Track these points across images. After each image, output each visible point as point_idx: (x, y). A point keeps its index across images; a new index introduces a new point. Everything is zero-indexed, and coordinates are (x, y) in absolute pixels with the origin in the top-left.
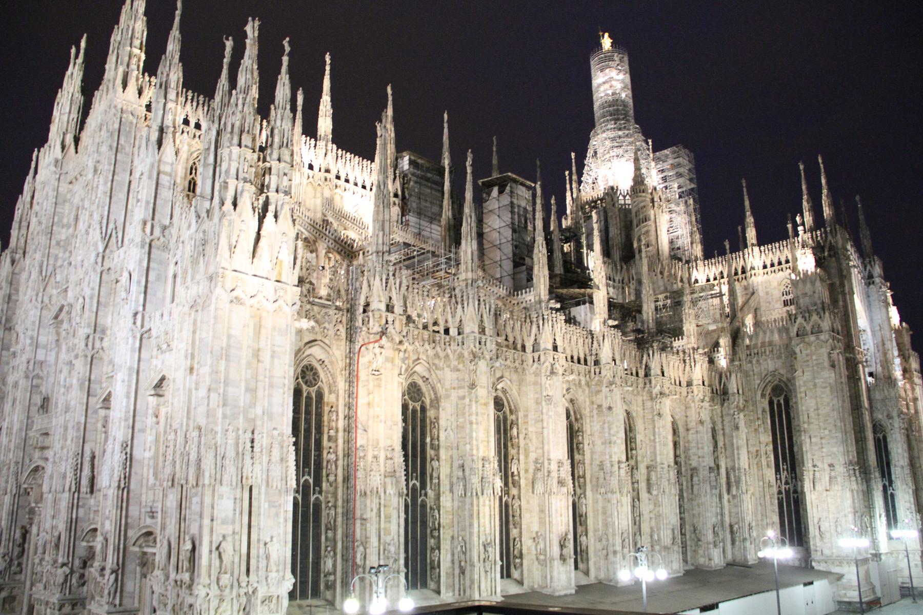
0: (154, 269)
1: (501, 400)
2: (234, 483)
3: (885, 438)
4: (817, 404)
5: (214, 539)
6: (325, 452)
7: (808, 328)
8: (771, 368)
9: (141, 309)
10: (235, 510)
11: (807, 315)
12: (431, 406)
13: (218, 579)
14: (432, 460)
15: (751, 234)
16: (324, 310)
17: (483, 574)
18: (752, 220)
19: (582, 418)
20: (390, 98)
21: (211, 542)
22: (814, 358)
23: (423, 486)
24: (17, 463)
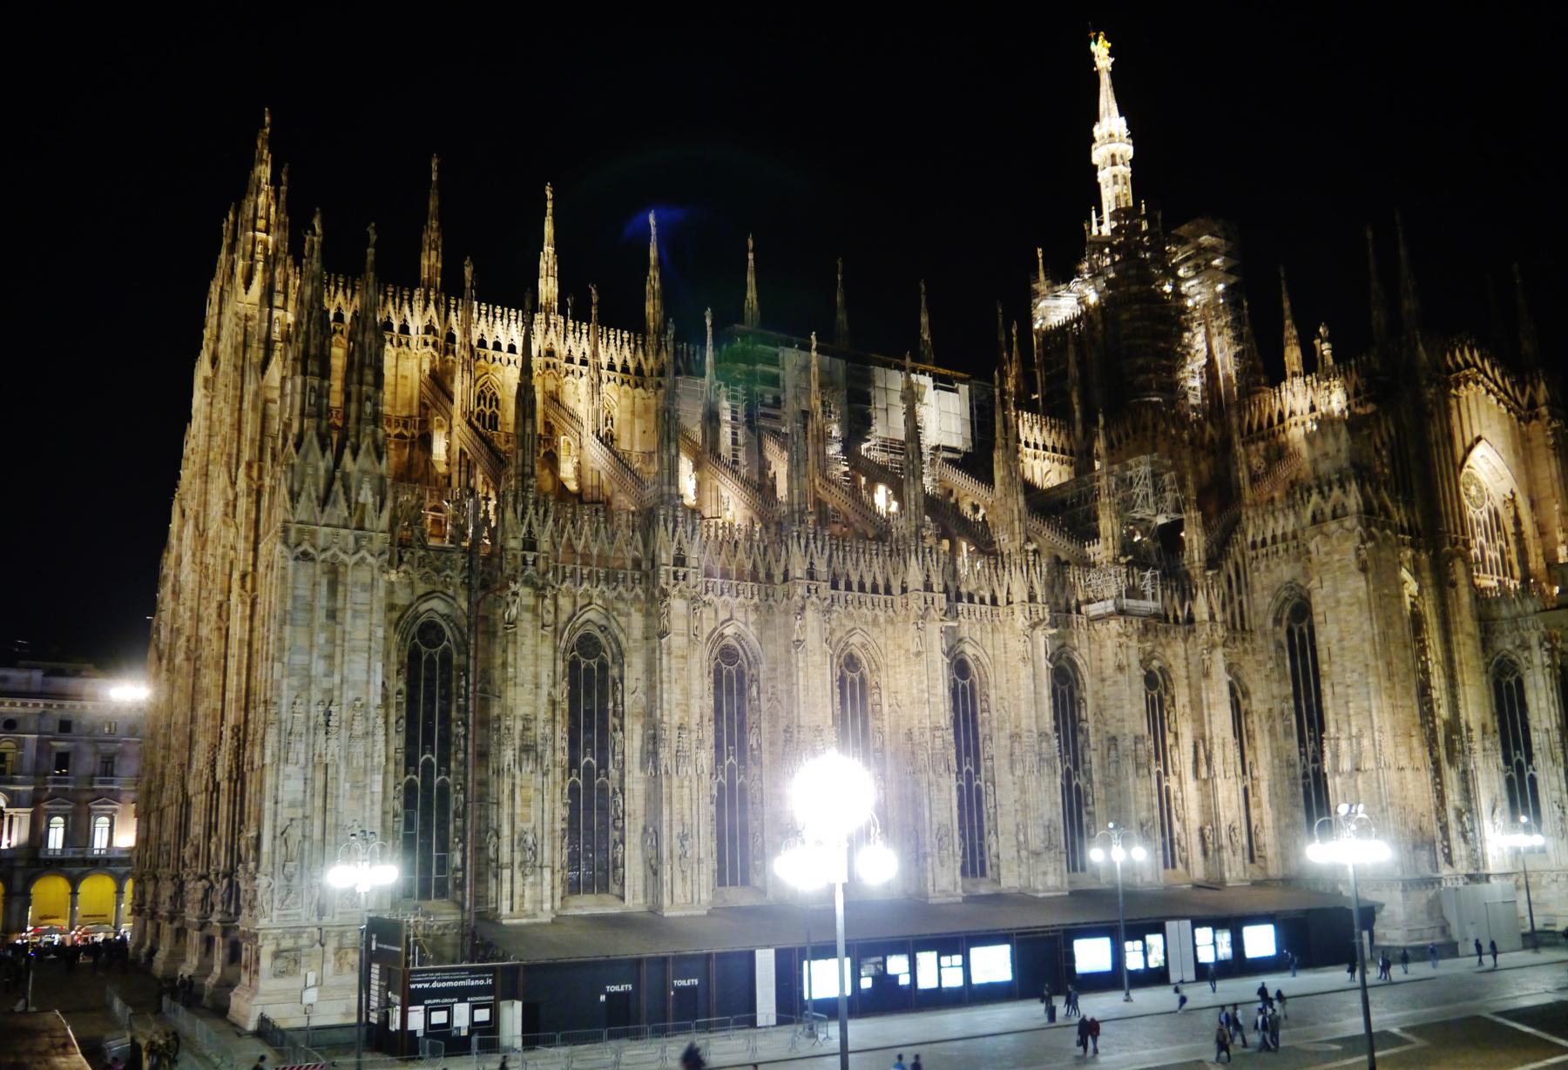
3: (1520, 683)
4: (1341, 631)
7: (1328, 510)
8: (1287, 577)
11: (1326, 489)
16: (444, 556)
17: (678, 876)
21: (275, 827)
23: (603, 764)
24: (182, 765)
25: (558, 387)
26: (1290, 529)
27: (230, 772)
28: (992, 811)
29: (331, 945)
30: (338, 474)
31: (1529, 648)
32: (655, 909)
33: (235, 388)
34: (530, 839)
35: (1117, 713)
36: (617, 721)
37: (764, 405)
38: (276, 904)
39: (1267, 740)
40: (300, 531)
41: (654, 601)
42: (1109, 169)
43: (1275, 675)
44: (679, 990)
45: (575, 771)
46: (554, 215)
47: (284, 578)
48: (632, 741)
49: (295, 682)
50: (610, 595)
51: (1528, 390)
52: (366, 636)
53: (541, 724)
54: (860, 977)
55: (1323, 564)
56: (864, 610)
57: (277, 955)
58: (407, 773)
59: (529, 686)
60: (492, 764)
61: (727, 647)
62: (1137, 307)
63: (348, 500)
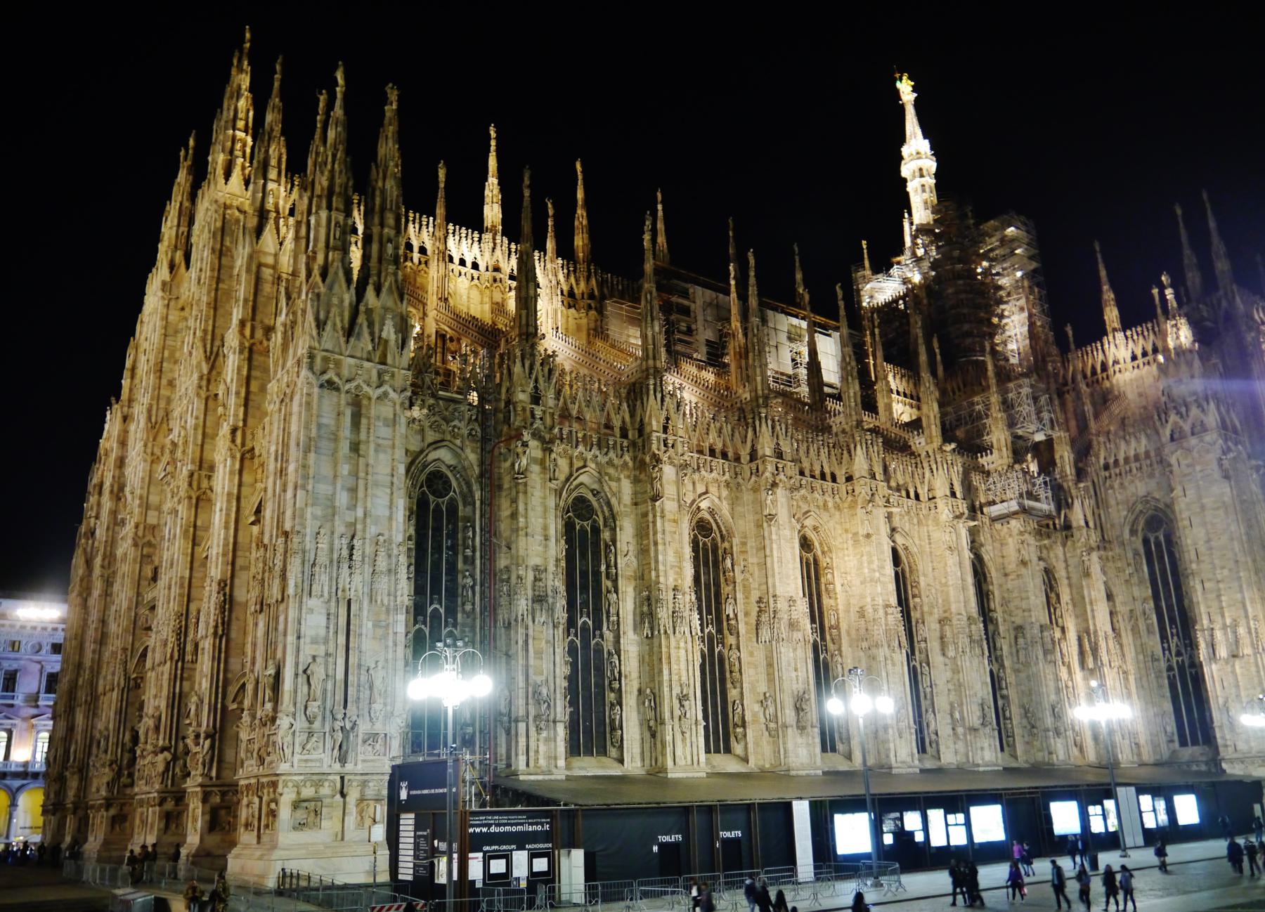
0: (256, 378)
1: (709, 523)
2: (326, 594)
4: (1207, 533)
5: (301, 659)
6: (460, 576)
7: (1187, 427)
9: (241, 424)
10: (328, 628)
11: (1183, 410)
12: (605, 526)
13: (306, 708)
14: (608, 592)
15: (1112, 315)
16: (452, 406)
17: (678, 736)
18: (1112, 296)
19: (830, 551)
20: (580, 177)
21: (297, 664)
22: (1198, 468)
23: (598, 625)
24: (125, 650)
25: (504, 300)
26: (1142, 450)
27: (216, 627)
28: (928, 690)
29: (353, 796)
30: (362, 308)
32: (656, 774)
33: (212, 270)
34: (544, 691)
36: (609, 584)
37: (679, 332)
38: (298, 749)
39: (1131, 638)
40: (326, 360)
41: (645, 470)
43: (1135, 580)
44: (726, 842)
45: (572, 631)
46: (497, 151)
47: (308, 404)
48: (626, 603)
49: (319, 512)
52: (388, 471)
53: (551, 576)
54: (882, 832)
55: (1185, 475)
56: (816, 495)
57: (296, 805)
58: (416, 622)
59: (539, 538)
60: (502, 615)
61: (701, 520)
62: (961, 282)
63: (372, 334)
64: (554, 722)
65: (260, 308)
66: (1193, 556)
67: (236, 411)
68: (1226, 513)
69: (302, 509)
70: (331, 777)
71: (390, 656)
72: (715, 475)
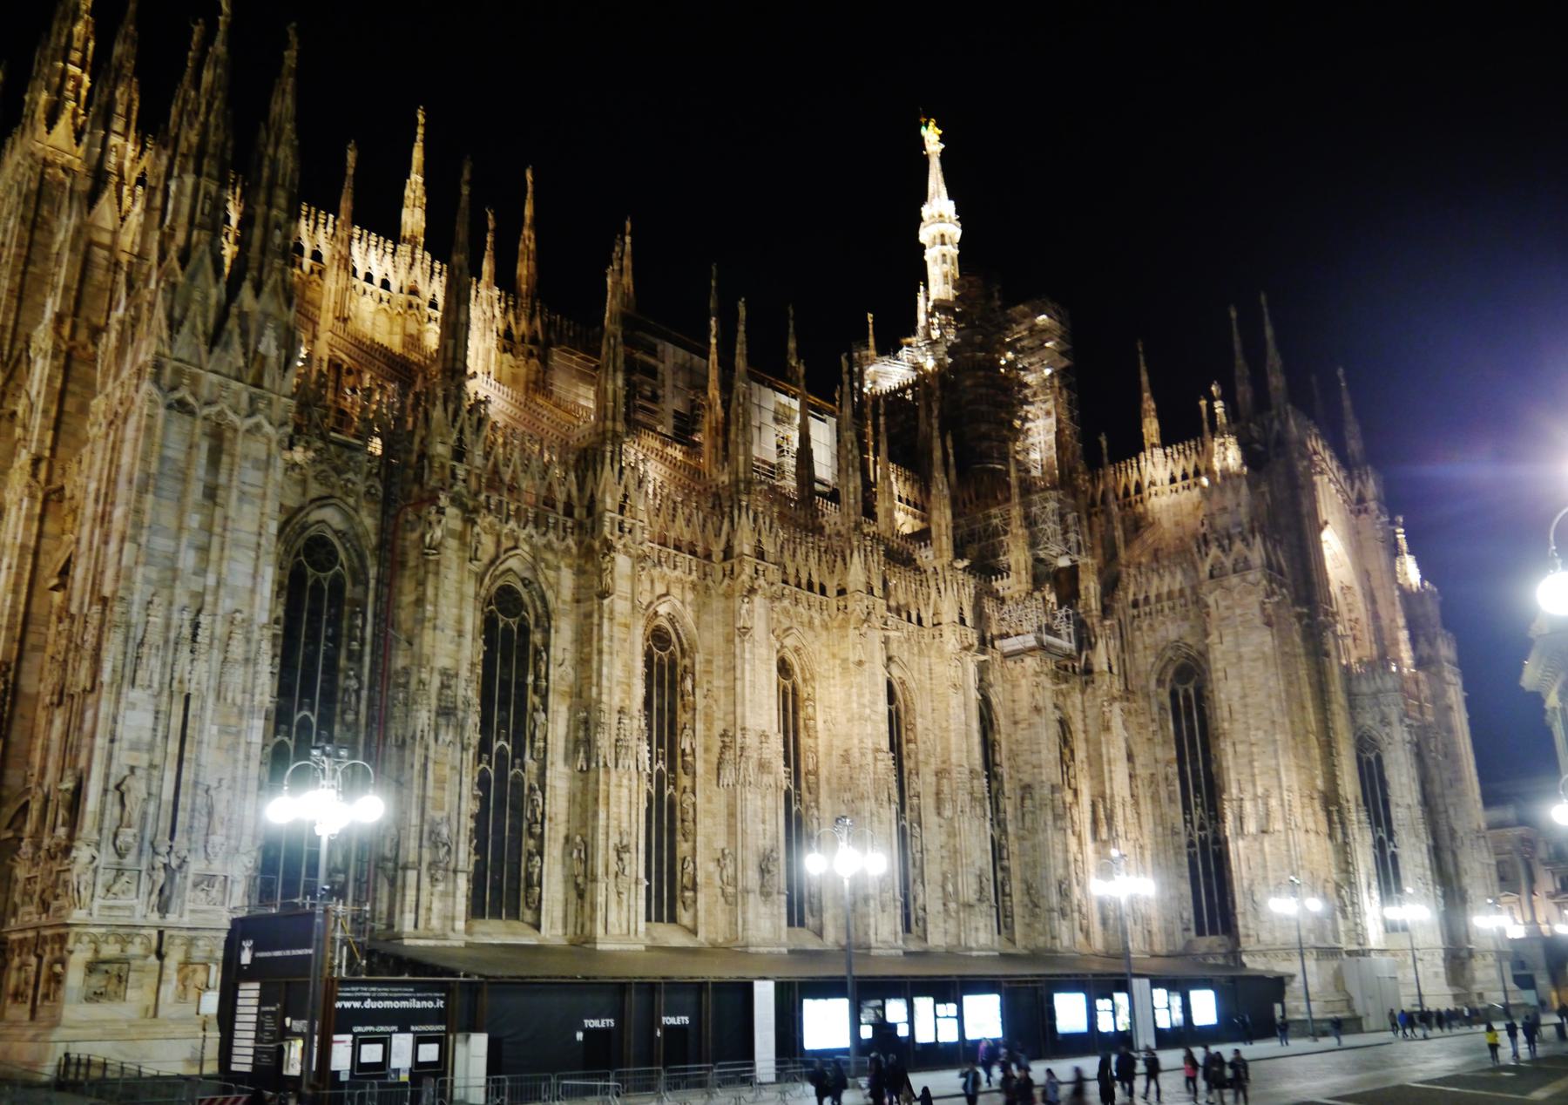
0: (74, 394)
1: (667, 633)
2: (156, 685)
3: (1379, 759)
5: (114, 769)
6: (341, 677)
7: (1228, 563)
8: (1173, 636)
9: (47, 453)
10: (155, 730)
11: (1226, 542)
12: (537, 625)
13: (116, 836)
14: (535, 709)
15: (1151, 428)
17: (613, 897)
18: (1153, 406)
19: (813, 678)
20: (530, 188)
21: (107, 777)
22: (1238, 611)
25: (420, 332)
26: (1177, 587)
28: (918, 856)
29: (174, 957)
30: (234, 310)
31: (1389, 724)
32: (582, 943)
33: (19, 245)
34: (445, 831)
35: (1034, 759)
36: (537, 700)
37: (642, 397)
38: (100, 890)
39: (1149, 806)
40: (178, 372)
41: (592, 555)
42: (938, 247)
43: (1158, 739)
44: (669, 1029)
45: (485, 756)
46: (425, 141)
47: (149, 429)
48: (557, 725)
49: (153, 574)
50: (539, 541)
51: (1357, 484)
52: (255, 528)
53: (463, 684)
55: (1223, 619)
56: (800, 609)
57: (91, 968)
58: (277, 732)
59: (451, 633)
60: (395, 729)
61: (658, 628)
62: (981, 373)
63: (245, 345)
64: (455, 871)
65: (87, 300)
66: (1226, 714)
67: (41, 435)
68: (1266, 664)
69: (129, 569)
70: (144, 931)
71: (240, 772)
72: (682, 571)
